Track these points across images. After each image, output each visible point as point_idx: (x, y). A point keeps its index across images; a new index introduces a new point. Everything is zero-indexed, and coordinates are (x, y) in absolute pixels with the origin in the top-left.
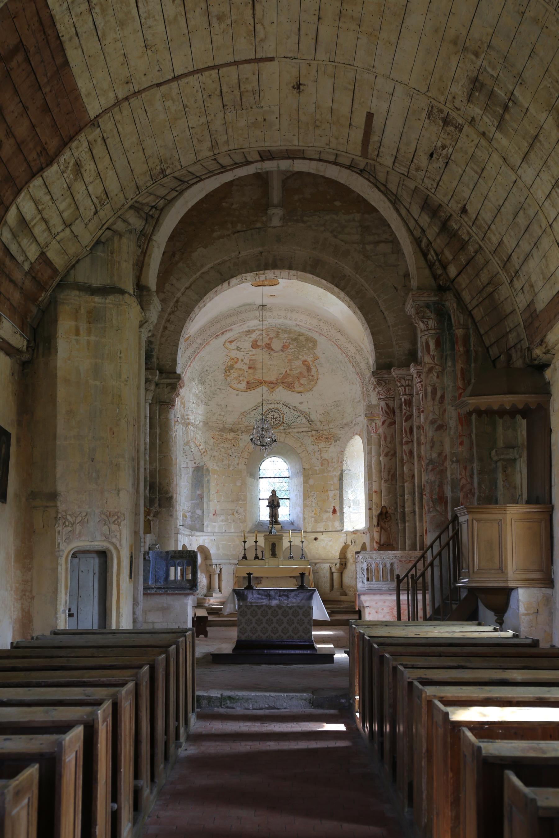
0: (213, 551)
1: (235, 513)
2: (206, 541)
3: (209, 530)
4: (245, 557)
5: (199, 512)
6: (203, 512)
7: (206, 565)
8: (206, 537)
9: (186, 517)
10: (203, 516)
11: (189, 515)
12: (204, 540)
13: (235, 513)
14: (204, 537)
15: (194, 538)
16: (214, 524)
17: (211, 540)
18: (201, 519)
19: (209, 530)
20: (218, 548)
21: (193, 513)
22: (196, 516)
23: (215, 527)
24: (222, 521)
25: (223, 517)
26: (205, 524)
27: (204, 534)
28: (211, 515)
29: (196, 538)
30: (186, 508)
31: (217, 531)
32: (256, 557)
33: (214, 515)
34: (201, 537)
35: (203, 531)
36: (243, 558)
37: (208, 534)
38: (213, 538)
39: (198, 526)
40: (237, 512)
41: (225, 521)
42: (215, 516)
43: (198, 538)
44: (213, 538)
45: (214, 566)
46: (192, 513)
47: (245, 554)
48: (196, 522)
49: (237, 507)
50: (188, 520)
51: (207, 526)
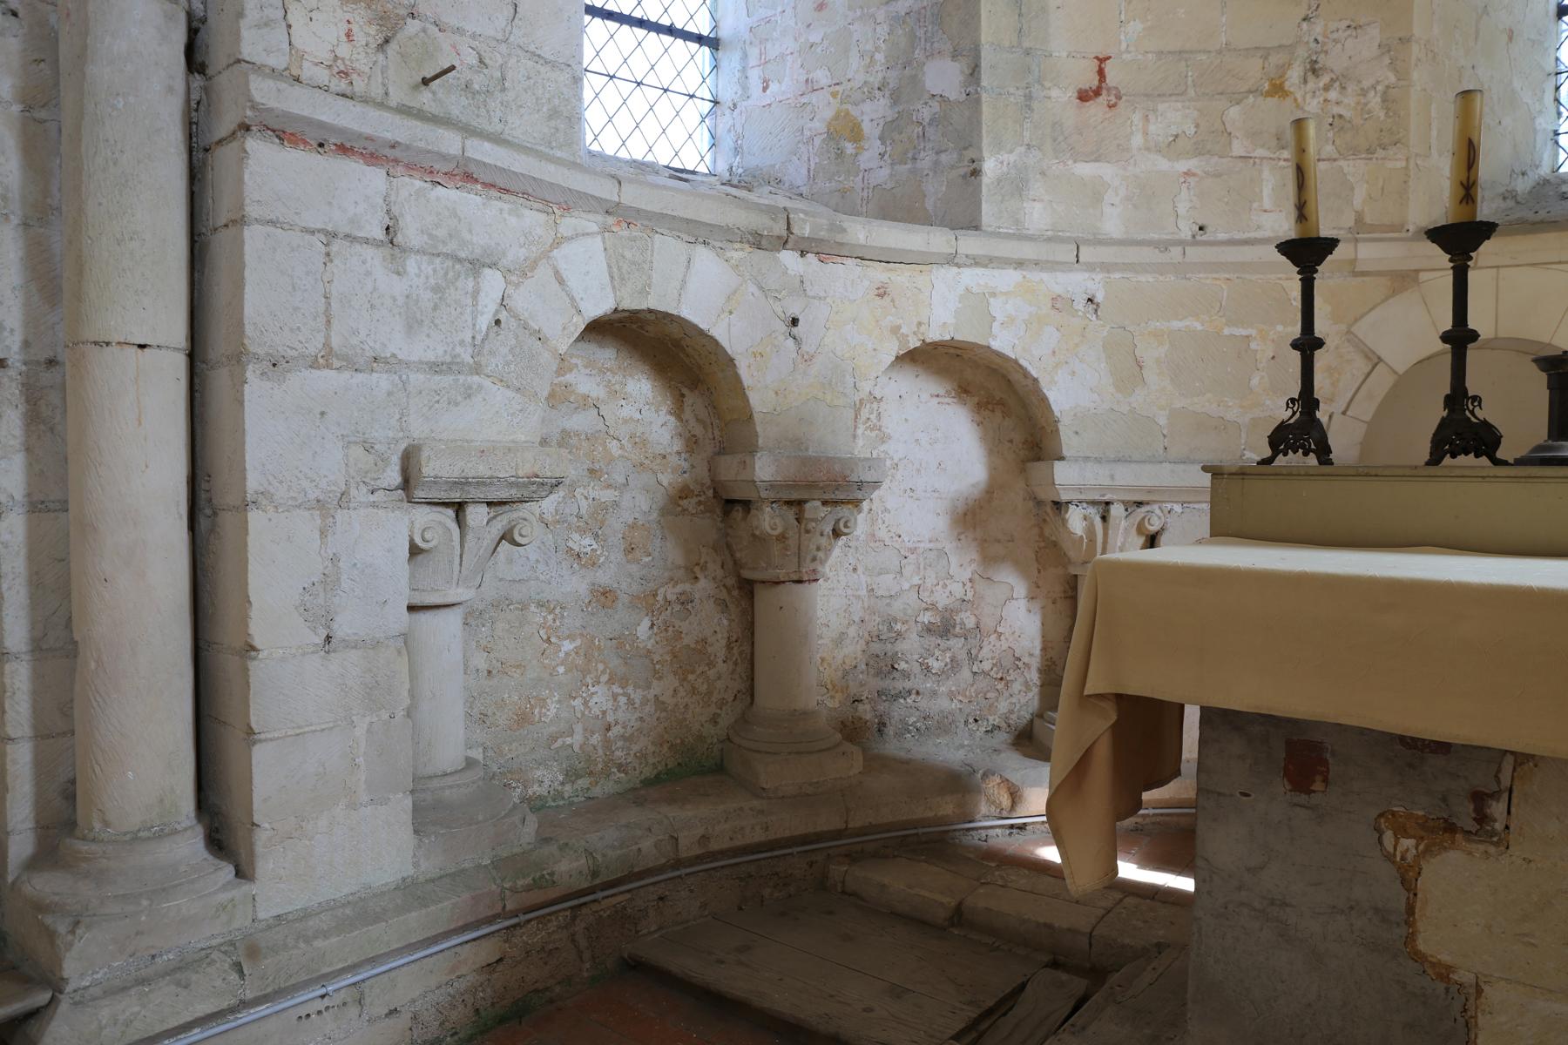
0: (1068, 393)
1: (1294, 75)
2: (997, 307)
3: (1037, 216)
4: (1301, 431)
5: (943, 77)
6: (974, 72)
7: (1039, 503)
8: (1007, 279)
9: (856, 134)
10: (973, 100)
11: (873, 114)
12: (977, 302)
13: (1294, 75)
14: (972, 277)
15: (843, 281)
16: (1085, 169)
17: (1060, 303)
18: (960, 130)
19: (1037, 216)
20: (1129, 372)
21: (902, 90)
22: (926, 114)
23: (1095, 193)
24: (1172, 146)
25: (1174, 118)
26: (990, 167)
27: (970, 244)
28: (1061, 97)
29: (878, 273)
30: (855, 62)
31: (1112, 223)
32: (1463, 434)
33: (1084, 96)
34: (944, 276)
35: (973, 225)
36: (1281, 439)
37: (1028, 251)
38: (1077, 283)
39: (935, 190)
40: (1314, 69)
41: (1199, 151)
42: (1096, 108)
43: (900, 277)
44: (1077, 283)
45: (1076, 521)
46: (896, 98)
47: (1307, 400)
48: (926, 160)
49: (1318, 29)
50: (869, 156)
51: (1017, 185)
